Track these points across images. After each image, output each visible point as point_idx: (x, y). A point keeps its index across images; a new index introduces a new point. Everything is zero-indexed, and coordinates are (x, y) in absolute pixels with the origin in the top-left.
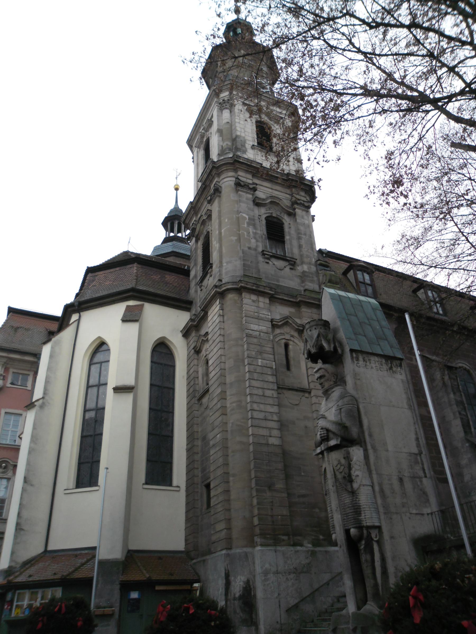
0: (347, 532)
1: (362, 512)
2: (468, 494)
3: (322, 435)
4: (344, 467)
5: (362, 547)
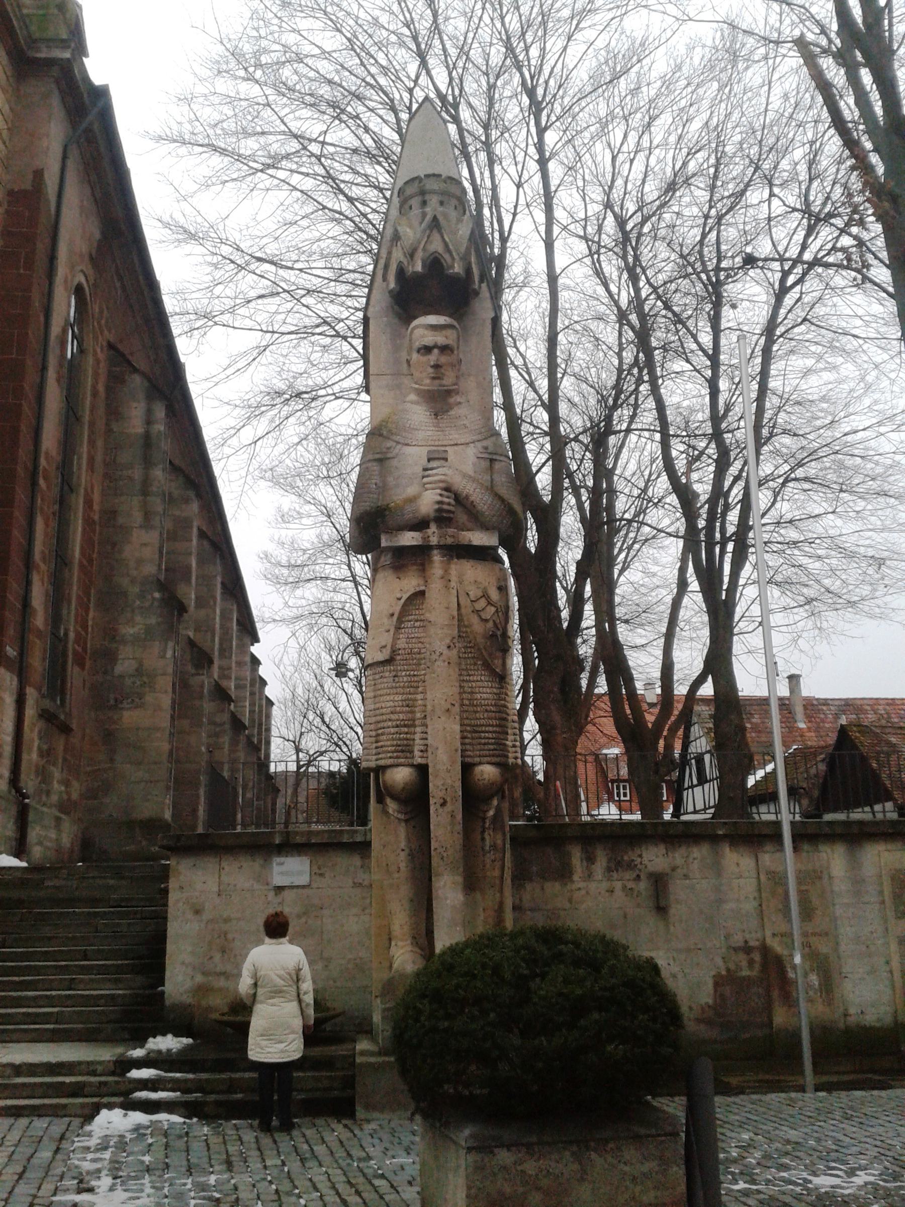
0: (467, 769)
1: (510, 731)
2: (112, 702)
3: (445, 507)
4: (497, 611)
5: (491, 813)
